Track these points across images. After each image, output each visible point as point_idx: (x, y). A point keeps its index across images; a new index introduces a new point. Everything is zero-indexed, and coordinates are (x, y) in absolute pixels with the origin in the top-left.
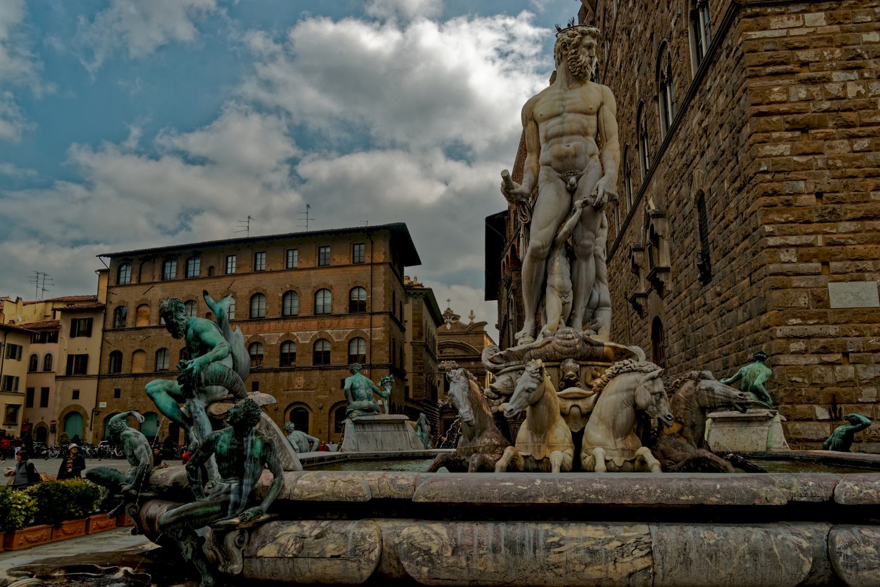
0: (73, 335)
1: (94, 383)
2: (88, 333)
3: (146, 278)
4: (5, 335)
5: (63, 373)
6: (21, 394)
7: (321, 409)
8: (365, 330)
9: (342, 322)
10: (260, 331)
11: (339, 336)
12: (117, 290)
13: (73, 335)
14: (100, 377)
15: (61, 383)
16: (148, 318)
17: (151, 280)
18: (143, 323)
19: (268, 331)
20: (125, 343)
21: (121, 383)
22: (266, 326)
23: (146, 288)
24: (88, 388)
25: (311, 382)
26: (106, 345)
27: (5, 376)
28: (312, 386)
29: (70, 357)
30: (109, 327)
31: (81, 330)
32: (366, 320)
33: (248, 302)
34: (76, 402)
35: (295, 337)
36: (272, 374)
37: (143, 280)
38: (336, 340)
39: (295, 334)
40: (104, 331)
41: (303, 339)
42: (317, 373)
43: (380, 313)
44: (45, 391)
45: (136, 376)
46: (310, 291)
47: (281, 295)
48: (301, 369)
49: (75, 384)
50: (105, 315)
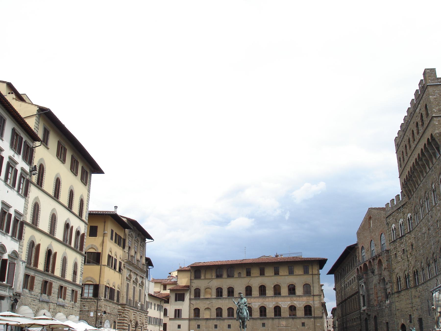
0: (176, 300)
1: (187, 322)
5: (173, 317)
8: (311, 302)
9: (301, 299)
11: (300, 304)
13: (176, 300)
14: (190, 319)
15: (172, 321)
16: (211, 294)
17: (211, 278)
18: (209, 296)
20: (200, 304)
21: (200, 323)
23: (209, 281)
28: (289, 325)
31: (180, 297)
32: (311, 298)
37: (207, 277)
38: (298, 306)
40: (190, 299)
42: (291, 320)
43: (317, 295)
45: (207, 319)
48: (284, 318)
49: (178, 322)
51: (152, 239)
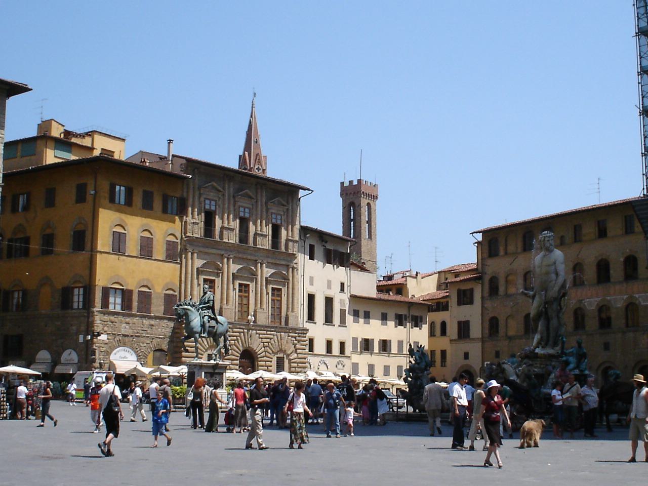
2: (471, 302)
3: (511, 248)
5: (455, 336)
12: (490, 262)
24: (475, 349)
30: (486, 294)
31: (465, 298)
34: (467, 362)
35: (637, 299)
40: (483, 298)
44: (443, 353)
47: (622, 259)
49: (464, 346)
51: (309, 190)
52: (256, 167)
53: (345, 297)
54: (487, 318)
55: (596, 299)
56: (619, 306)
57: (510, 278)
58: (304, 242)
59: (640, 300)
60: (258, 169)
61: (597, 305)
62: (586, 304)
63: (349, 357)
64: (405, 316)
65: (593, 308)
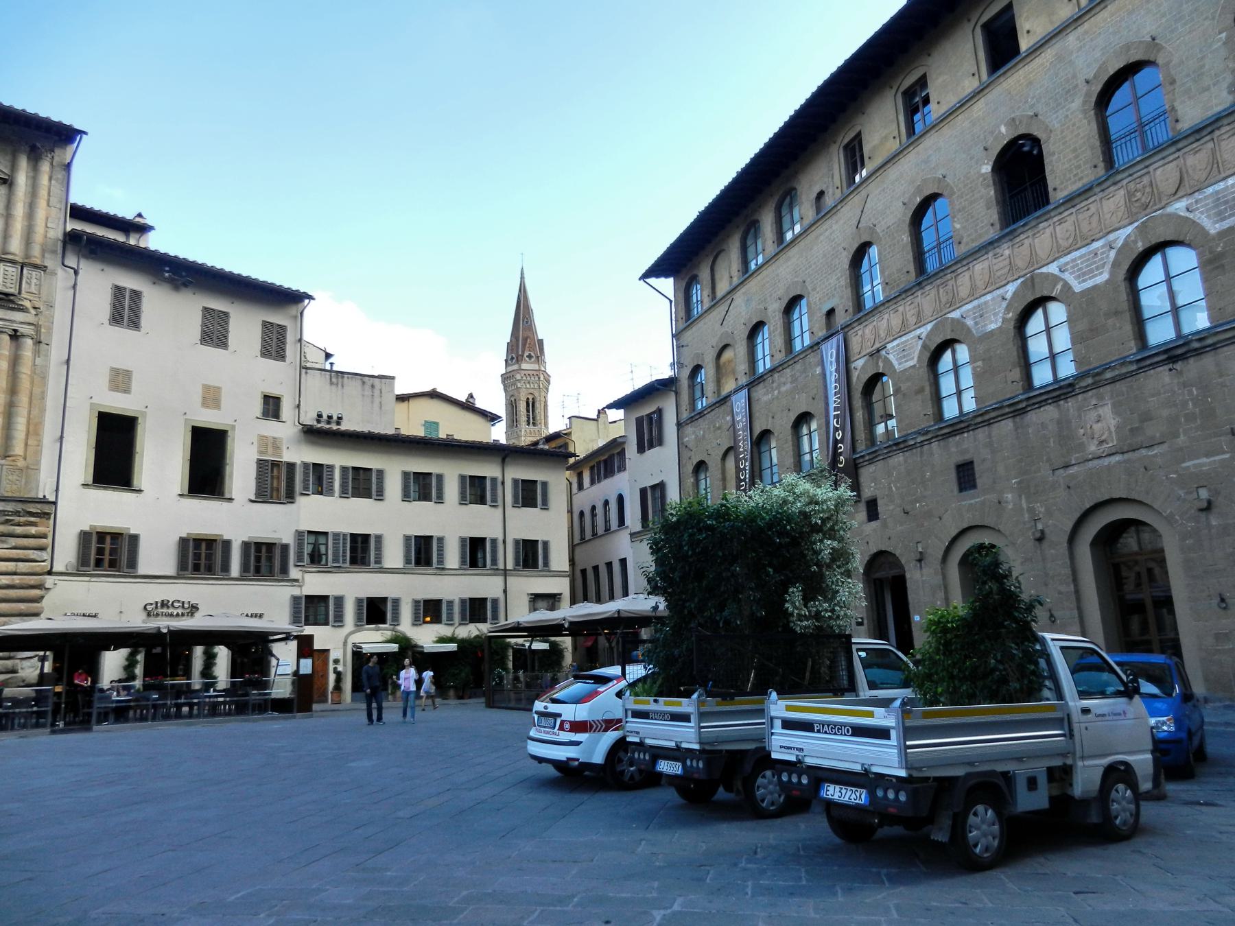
4: (503, 461)
6: (559, 574)
7: (1208, 507)
10: (953, 304)
19: (973, 295)
22: (963, 282)
25: (1146, 417)
26: (685, 454)
27: (517, 542)
28: (1154, 430)
29: (643, 492)
33: (906, 238)
36: (1007, 425)
39: (1053, 269)
40: (679, 425)
41: (1082, 276)
46: (1076, 104)
47: (987, 168)
50: (676, 393)
52: (527, 354)
53: (285, 429)
54: (690, 468)
55: (918, 332)
56: (993, 326)
57: (728, 355)
58: (76, 273)
59: (1067, 276)
60: (530, 357)
61: (924, 346)
62: (891, 357)
63: (296, 581)
64: (494, 480)
65: (911, 363)
